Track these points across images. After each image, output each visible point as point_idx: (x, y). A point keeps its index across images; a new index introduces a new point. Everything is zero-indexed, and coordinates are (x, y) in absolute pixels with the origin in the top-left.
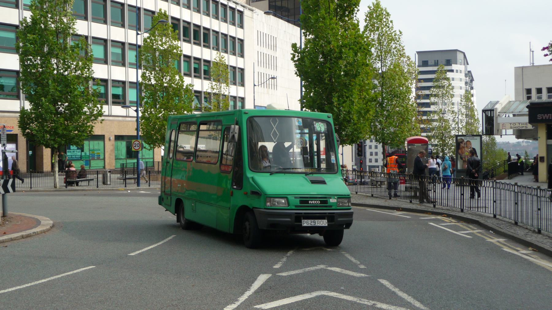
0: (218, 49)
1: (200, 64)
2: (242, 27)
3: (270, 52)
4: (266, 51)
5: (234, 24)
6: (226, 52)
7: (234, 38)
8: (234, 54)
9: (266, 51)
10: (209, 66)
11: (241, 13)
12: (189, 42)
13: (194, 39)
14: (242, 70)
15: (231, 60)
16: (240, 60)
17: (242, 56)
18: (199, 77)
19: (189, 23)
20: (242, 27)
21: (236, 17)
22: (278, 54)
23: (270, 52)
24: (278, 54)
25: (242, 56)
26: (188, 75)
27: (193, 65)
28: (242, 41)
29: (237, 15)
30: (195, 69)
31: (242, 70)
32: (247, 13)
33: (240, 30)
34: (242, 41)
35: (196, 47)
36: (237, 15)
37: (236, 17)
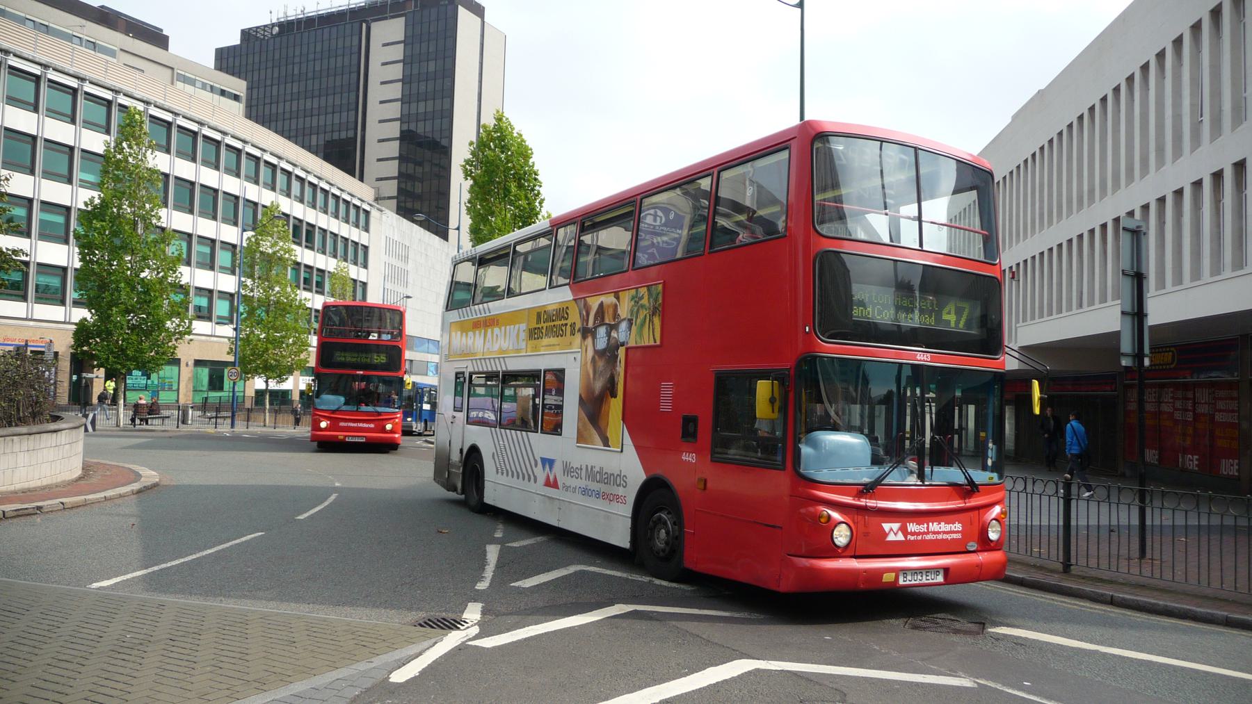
0: (335, 257)
1: (311, 274)
2: (367, 230)
3: (400, 264)
4: (394, 262)
5: (357, 226)
6: (346, 260)
7: (356, 244)
8: (356, 264)
9: (394, 262)
10: (323, 278)
11: (367, 213)
12: (299, 244)
13: (307, 241)
14: (364, 284)
15: (354, 272)
16: (363, 271)
17: (365, 267)
18: (310, 290)
19: (301, 221)
20: (367, 230)
21: (361, 218)
22: (410, 267)
23: (400, 264)
24: (410, 267)
25: (365, 267)
26: (298, 287)
27: (302, 275)
28: (366, 248)
29: (362, 216)
30: (305, 279)
31: (364, 284)
32: (374, 214)
33: (364, 234)
34: (366, 248)
35: (307, 251)
36: (362, 216)
37: (361, 218)
